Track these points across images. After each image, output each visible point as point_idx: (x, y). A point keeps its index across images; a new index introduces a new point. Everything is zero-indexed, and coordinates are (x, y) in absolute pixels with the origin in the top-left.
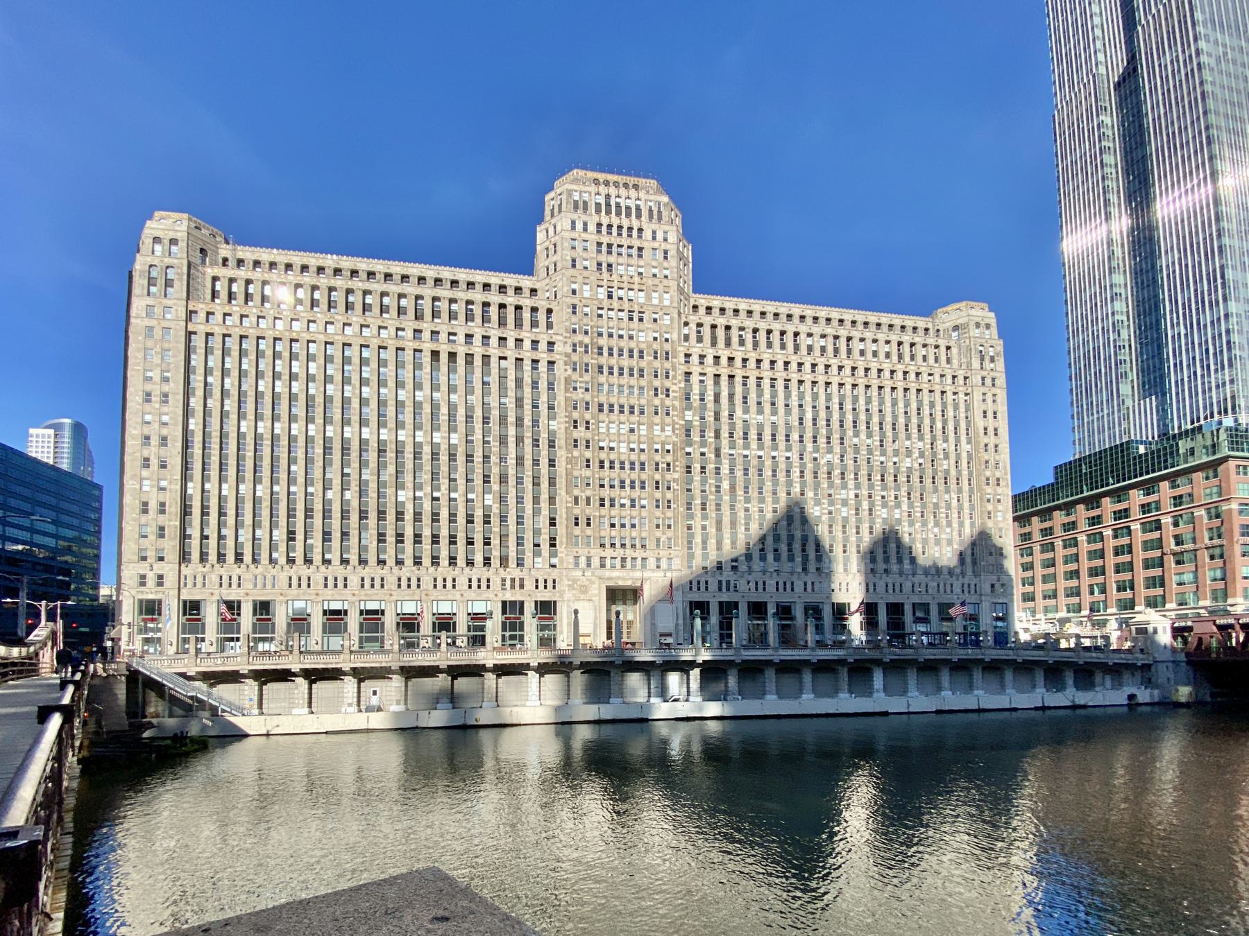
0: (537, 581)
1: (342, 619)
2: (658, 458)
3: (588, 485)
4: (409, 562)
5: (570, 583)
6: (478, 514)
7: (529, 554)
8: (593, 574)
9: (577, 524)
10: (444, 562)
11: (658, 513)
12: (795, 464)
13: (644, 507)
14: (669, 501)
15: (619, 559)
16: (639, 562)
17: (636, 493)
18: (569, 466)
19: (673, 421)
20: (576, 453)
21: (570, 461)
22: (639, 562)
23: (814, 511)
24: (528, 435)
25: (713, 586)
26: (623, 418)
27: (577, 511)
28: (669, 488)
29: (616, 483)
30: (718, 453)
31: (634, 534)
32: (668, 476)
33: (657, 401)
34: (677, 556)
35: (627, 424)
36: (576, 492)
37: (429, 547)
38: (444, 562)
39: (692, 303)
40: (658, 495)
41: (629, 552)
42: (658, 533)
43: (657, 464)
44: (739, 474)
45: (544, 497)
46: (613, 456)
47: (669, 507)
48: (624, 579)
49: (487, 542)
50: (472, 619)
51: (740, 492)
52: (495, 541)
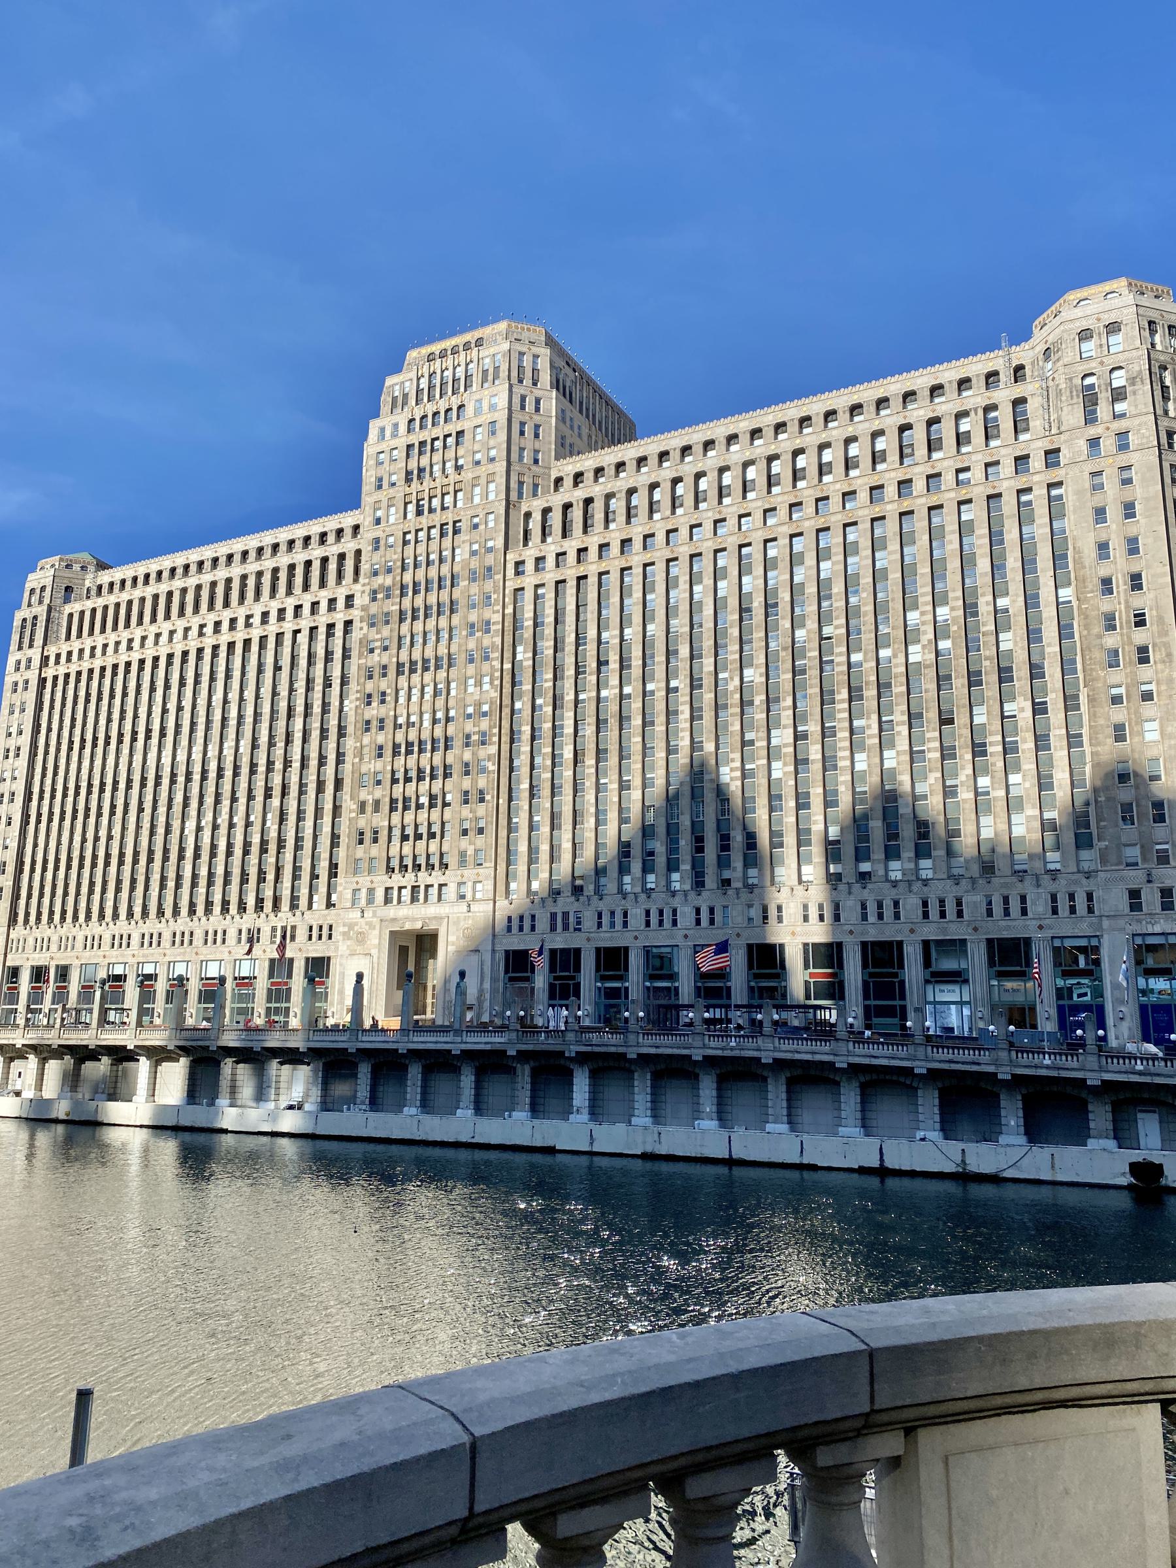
0: (311, 928)
1: (121, 987)
2: (469, 727)
3: (379, 783)
4: (184, 911)
5: (346, 929)
6: (256, 840)
7: (304, 892)
8: (374, 915)
9: (361, 842)
10: (217, 909)
11: (466, 811)
12: (681, 699)
13: (449, 805)
14: (481, 792)
15: (409, 888)
16: (434, 891)
17: (437, 786)
18: (357, 760)
19: (492, 667)
20: (366, 740)
21: (360, 753)
22: (434, 891)
23: (729, 775)
24: (315, 725)
25: (543, 924)
26: (428, 677)
27: (362, 823)
28: (483, 770)
29: (413, 774)
30: (556, 702)
31: (434, 846)
32: (483, 752)
33: (472, 644)
34: (487, 879)
35: (432, 685)
36: (364, 795)
37: (204, 890)
38: (217, 909)
39: (554, 475)
40: (467, 783)
41: (424, 878)
42: (464, 843)
43: (468, 736)
44: (589, 730)
45: (328, 807)
46: (413, 736)
47: (482, 800)
48: (414, 920)
49: (261, 878)
50: (237, 985)
51: (590, 761)
52: (270, 877)
